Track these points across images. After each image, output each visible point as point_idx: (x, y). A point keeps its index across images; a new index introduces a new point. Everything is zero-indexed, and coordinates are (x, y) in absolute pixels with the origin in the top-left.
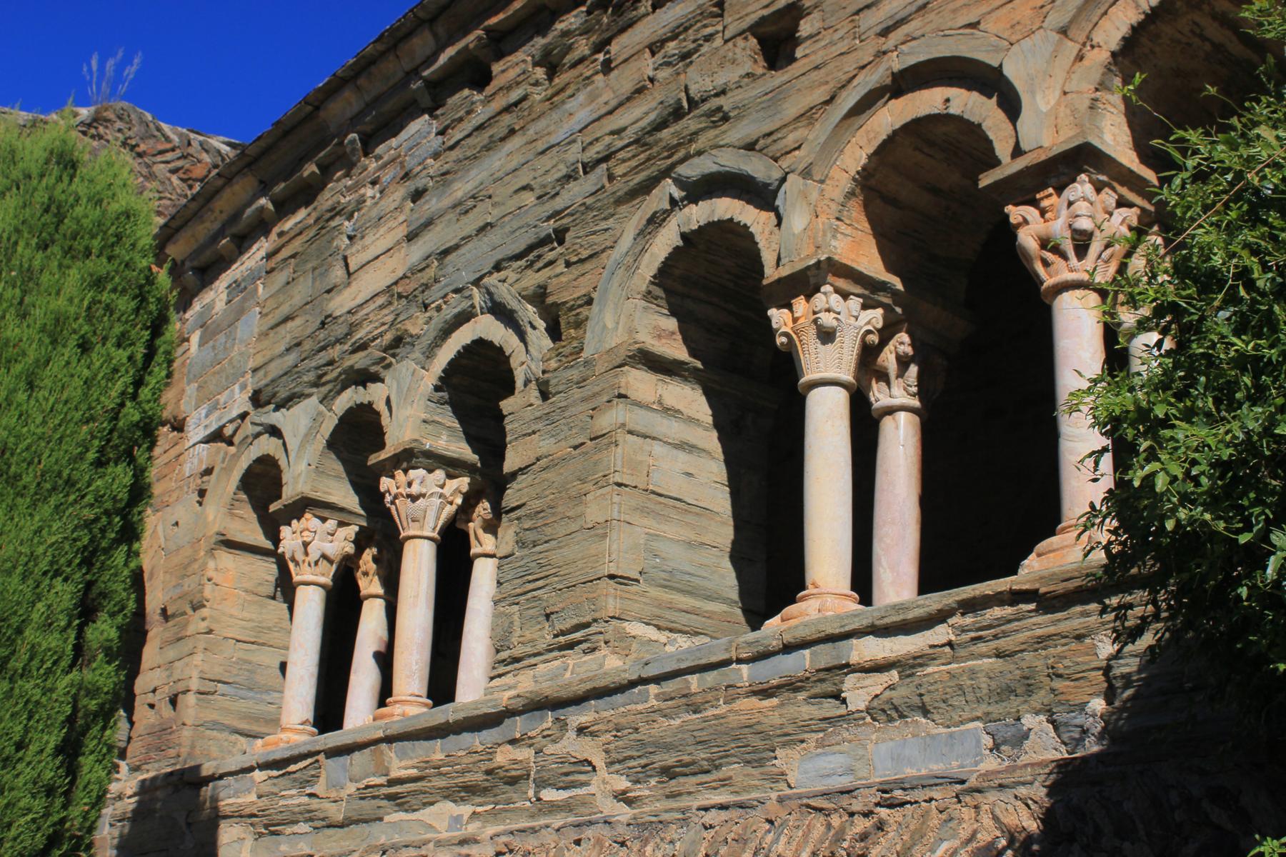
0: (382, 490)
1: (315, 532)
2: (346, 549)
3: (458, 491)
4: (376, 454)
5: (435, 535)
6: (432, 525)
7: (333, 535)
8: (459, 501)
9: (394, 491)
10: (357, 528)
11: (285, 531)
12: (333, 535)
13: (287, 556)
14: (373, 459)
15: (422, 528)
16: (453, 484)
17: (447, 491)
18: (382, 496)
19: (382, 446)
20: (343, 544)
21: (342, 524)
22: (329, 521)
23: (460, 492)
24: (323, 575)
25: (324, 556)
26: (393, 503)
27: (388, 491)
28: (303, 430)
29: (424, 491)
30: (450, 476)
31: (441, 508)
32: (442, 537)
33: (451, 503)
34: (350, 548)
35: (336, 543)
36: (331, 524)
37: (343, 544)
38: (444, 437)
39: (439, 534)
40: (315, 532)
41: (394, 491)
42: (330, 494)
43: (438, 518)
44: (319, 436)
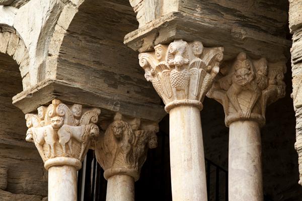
0: (142, 65)
1: (64, 116)
2: (92, 131)
3: (212, 62)
4: (133, 33)
5: (196, 102)
6: (195, 92)
7: (79, 118)
8: (216, 69)
9: (155, 63)
10: (99, 111)
11: (30, 119)
12: (79, 118)
13: (37, 143)
14: (129, 38)
15: (187, 96)
16: (211, 53)
17: (206, 60)
18: (142, 71)
19: (20, 89)
20: (88, 126)
21: (86, 107)
22: (75, 106)
23: (217, 61)
24: (74, 156)
25: (73, 138)
26: (153, 75)
27: (148, 66)
28: (39, 24)
29: (187, 61)
30: (207, 46)
31: (203, 76)
32: (203, 103)
33: (210, 72)
34: (94, 130)
35: (83, 126)
36: (76, 109)
37: (88, 126)
38: (198, 10)
39: (201, 101)
40: (64, 116)
41: (155, 63)
42: (74, 81)
43: (200, 86)
44: (57, 28)
